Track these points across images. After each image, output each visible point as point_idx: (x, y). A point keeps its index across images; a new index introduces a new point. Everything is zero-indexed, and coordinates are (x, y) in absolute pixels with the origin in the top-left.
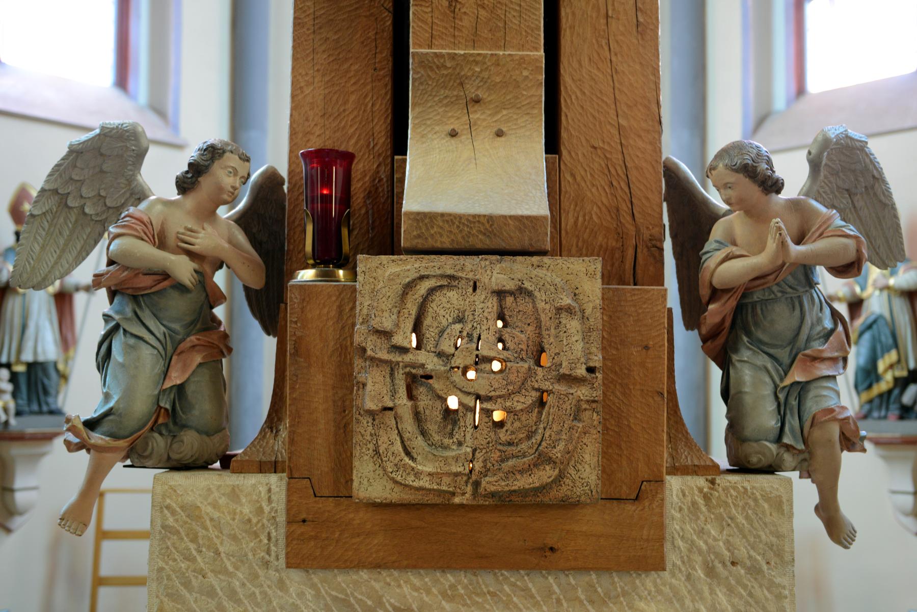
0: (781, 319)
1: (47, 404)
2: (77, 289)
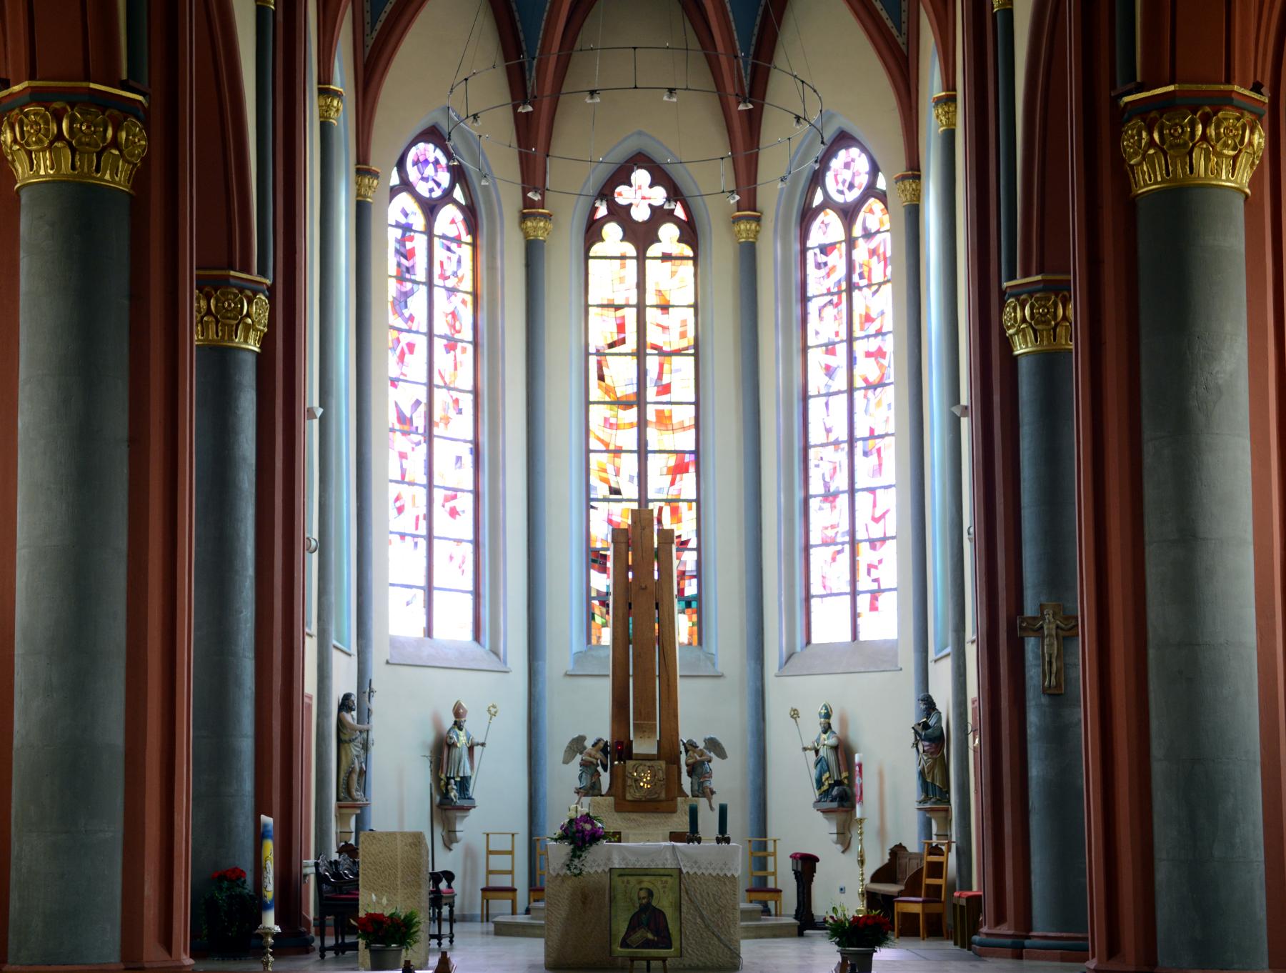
0: (699, 770)
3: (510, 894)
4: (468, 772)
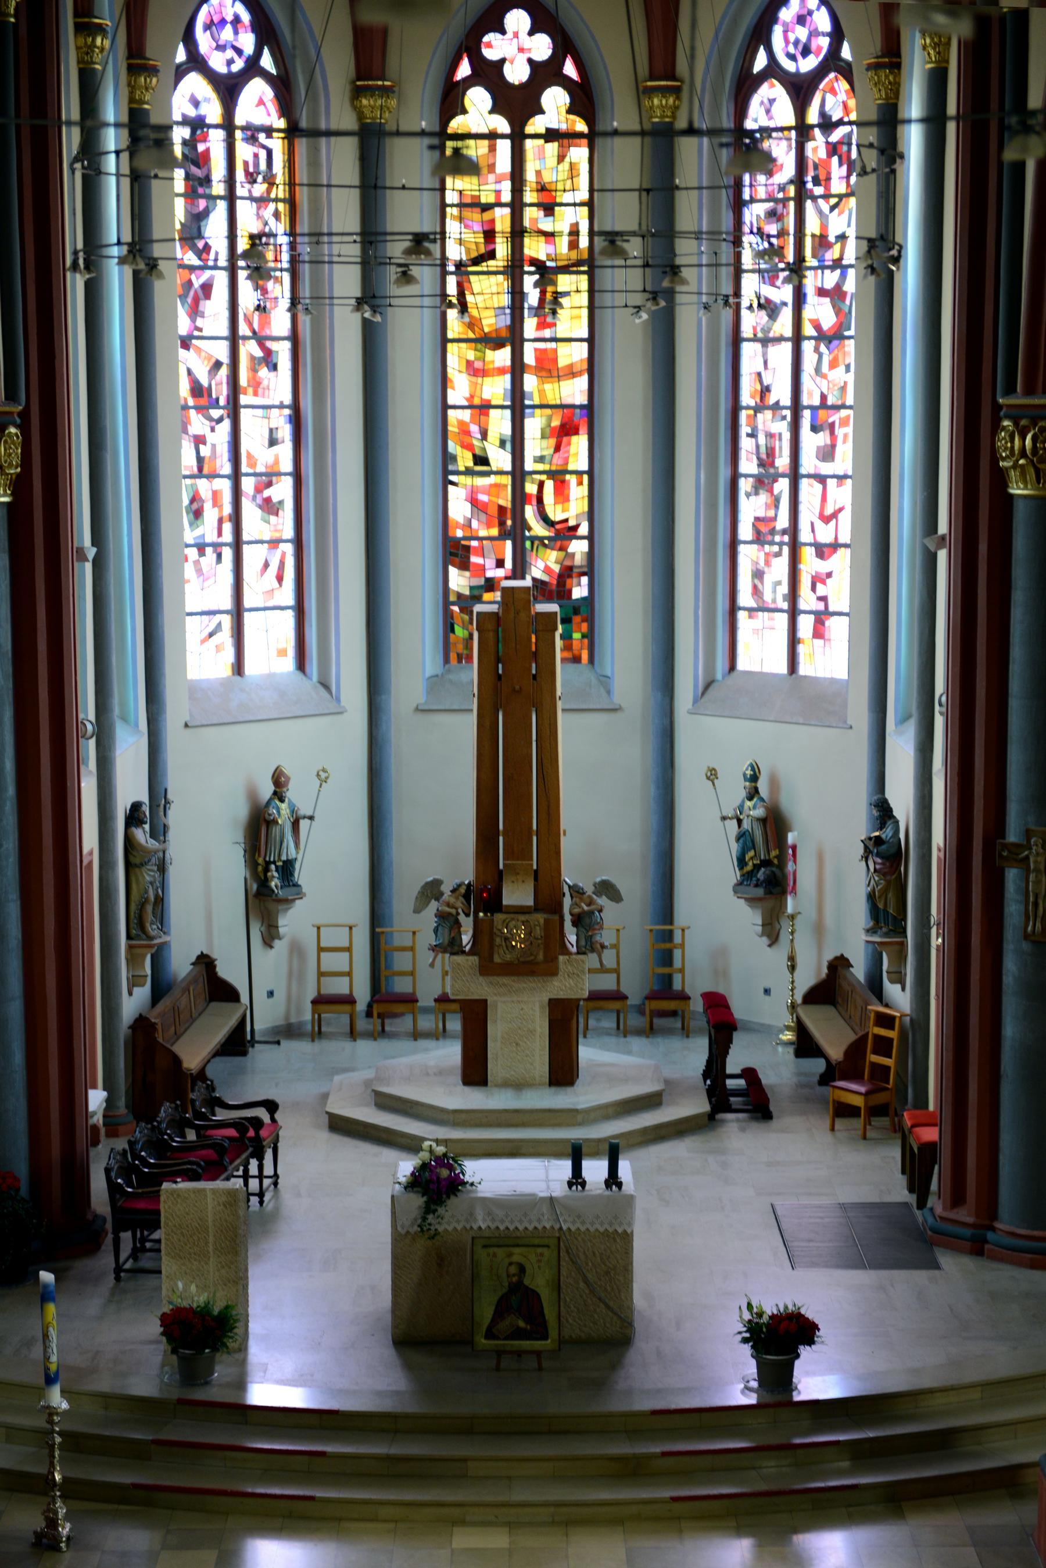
0: (587, 921)
2: (304, 817)
3: (347, 1008)
4: (293, 853)
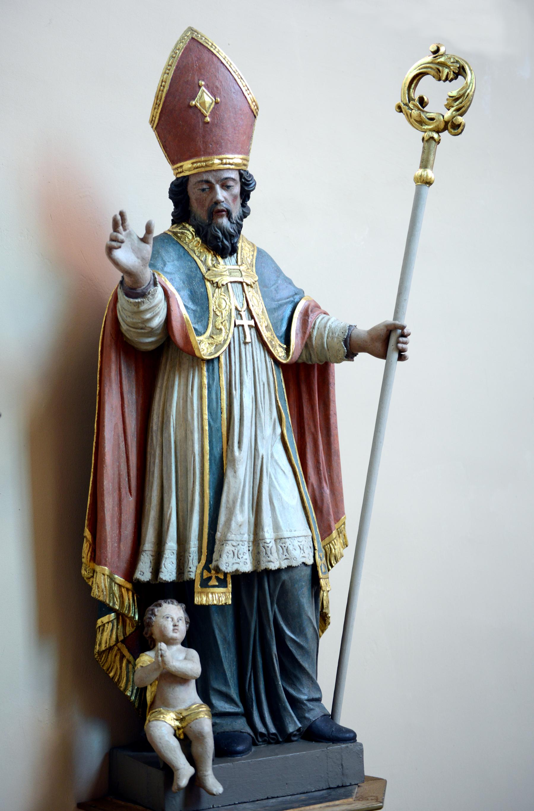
1: (295, 703)
2: (351, 348)
4: (292, 539)
